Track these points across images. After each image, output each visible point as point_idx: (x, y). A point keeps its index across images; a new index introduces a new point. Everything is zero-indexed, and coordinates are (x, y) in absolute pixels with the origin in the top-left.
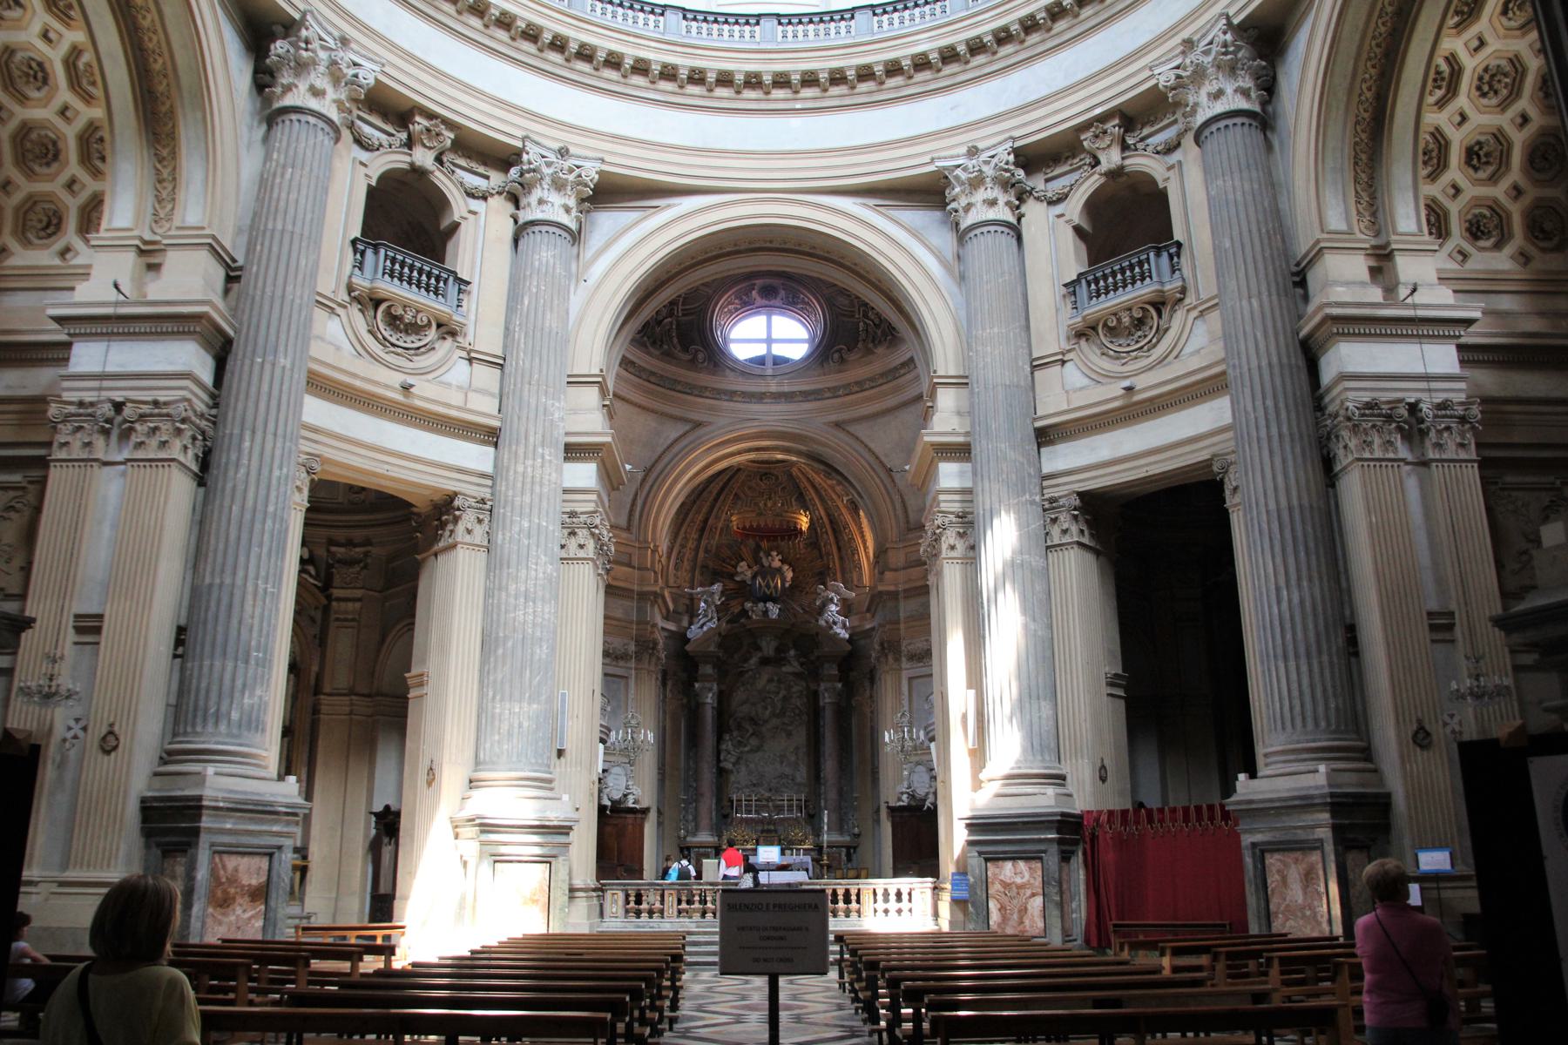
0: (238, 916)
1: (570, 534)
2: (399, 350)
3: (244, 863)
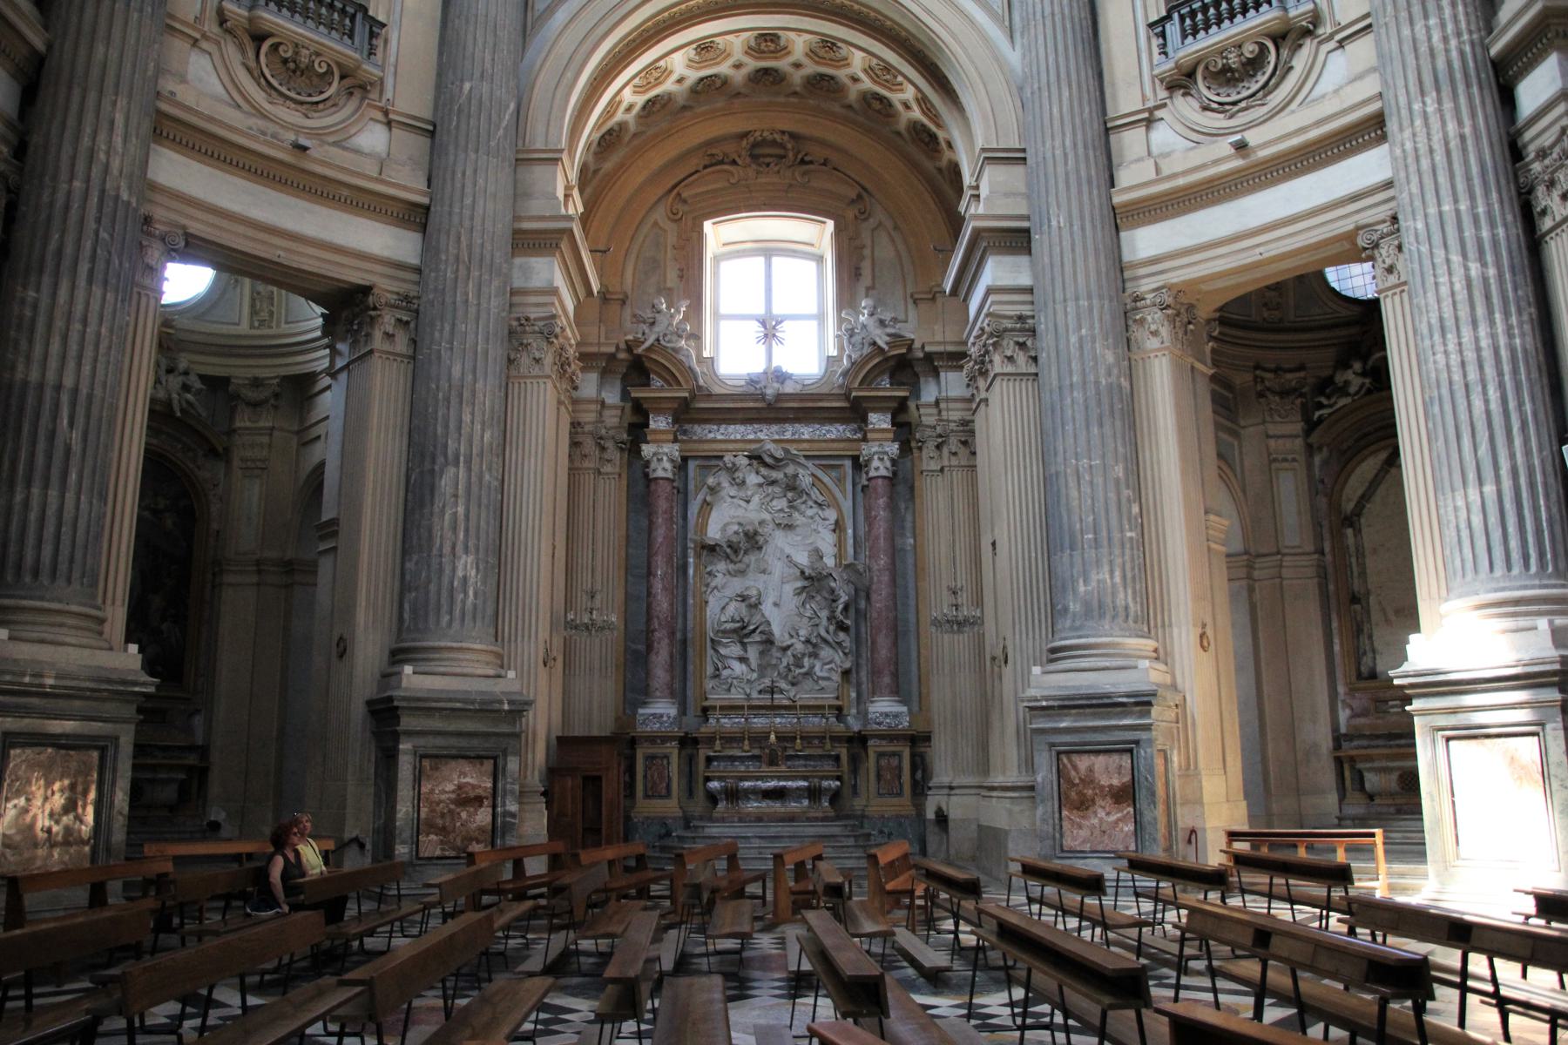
0: (1101, 820)
1: (1547, 187)
2: (1243, 104)
3: (1100, 762)
